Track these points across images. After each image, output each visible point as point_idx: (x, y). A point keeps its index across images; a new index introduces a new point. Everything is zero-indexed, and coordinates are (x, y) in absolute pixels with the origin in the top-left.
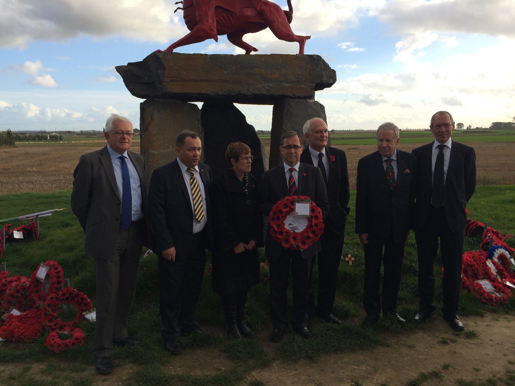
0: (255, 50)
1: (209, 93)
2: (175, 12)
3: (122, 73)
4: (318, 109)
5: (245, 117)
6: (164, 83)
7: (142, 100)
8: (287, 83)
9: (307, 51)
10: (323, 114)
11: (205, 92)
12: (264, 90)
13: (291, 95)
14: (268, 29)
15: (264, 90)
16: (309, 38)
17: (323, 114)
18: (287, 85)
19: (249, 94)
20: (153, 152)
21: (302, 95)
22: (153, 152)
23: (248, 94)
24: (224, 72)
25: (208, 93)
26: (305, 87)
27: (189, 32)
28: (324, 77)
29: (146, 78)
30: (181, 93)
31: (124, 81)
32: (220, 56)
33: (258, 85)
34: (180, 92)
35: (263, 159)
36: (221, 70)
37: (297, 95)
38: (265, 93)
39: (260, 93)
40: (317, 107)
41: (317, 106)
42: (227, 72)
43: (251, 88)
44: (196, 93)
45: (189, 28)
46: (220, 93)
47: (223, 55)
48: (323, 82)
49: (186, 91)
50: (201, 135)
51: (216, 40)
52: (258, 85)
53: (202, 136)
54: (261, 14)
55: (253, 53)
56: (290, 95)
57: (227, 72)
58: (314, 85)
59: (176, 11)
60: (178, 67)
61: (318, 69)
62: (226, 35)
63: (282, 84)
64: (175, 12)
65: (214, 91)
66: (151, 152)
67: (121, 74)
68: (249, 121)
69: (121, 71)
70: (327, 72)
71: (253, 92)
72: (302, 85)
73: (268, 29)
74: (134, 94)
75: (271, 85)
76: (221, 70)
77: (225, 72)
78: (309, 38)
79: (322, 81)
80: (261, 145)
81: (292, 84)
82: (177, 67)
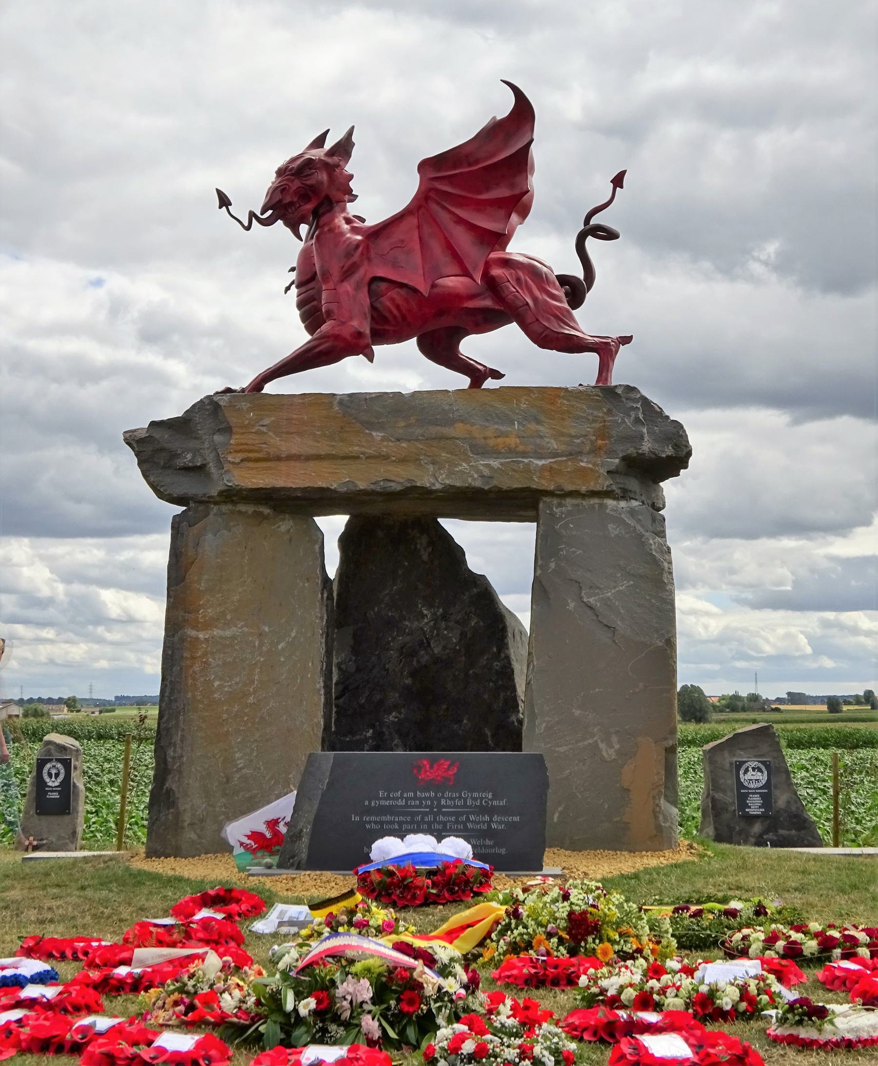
0: (497, 375)
1: (334, 486)
2: (286, 292)
3: (135, 445)
4: (643, 526)
5: (464, 554)
6: (227, 467)
7: (179, 509)
8: (540, 458)
9: (618, 377)
10: (654, 539)
11: (324, 485)
12: (476, 476)
13: (552, 488)
14: (515, 323)
15: (476, 476)
16: (626, 340)
17: (654, 539)
18: (540, 463)
19: (438, 486)
20: (193, 633)
21: (583, 489)
22: (193, 633)
23: (434, 488)
24: (374, 434)
25: (333, 488)
26: (590, 466)
27: (307, 337)
28: (646, 440)
29: (189, 456)
30: (266, 489)
31: (140, 464)
32: (368, 397)
33: (461, 465)
34: (264, 487)
35: (513, 672)
36: (367, 432)
37: (570, 487)
38: (478, 484)
39: (467, 485)
40: (639, 520)
41: (640, 517)
42: (383, 434)
43: (442, 472)
44: (302, 486)
45: (311, 329)
46: (362, 486)
47: (374, 396)
48: (643, 454)
49: (279, 482)
50: (322, 594)
51: (370, 357)
52: (461, 465)
53: (322, 597)
54: (492, 285)
55: (490, 384)
56: (549, 489)
57: (383, 434)
58: (617, 461)
59: (288, 289)
60: (263, 426)
61: (626, 420)
62: (414, 341)
63: (526, 461)
64: (286, 292)
65: (348, 481)
66: (189, 633)
67: (133, 448)
68: (475, 563)
69: (133, 442)
70: (656, 428)
71: (447, 482)
72: (582, 461)
73: (514, 326)
74: (161, 495)
75: (495, 463)
76: (367, 432)
77: (378, 436)
78: (626, 340)
79: (640, 451)
80: (510, 631)
81: (553, 460)
82: (261, 428)
